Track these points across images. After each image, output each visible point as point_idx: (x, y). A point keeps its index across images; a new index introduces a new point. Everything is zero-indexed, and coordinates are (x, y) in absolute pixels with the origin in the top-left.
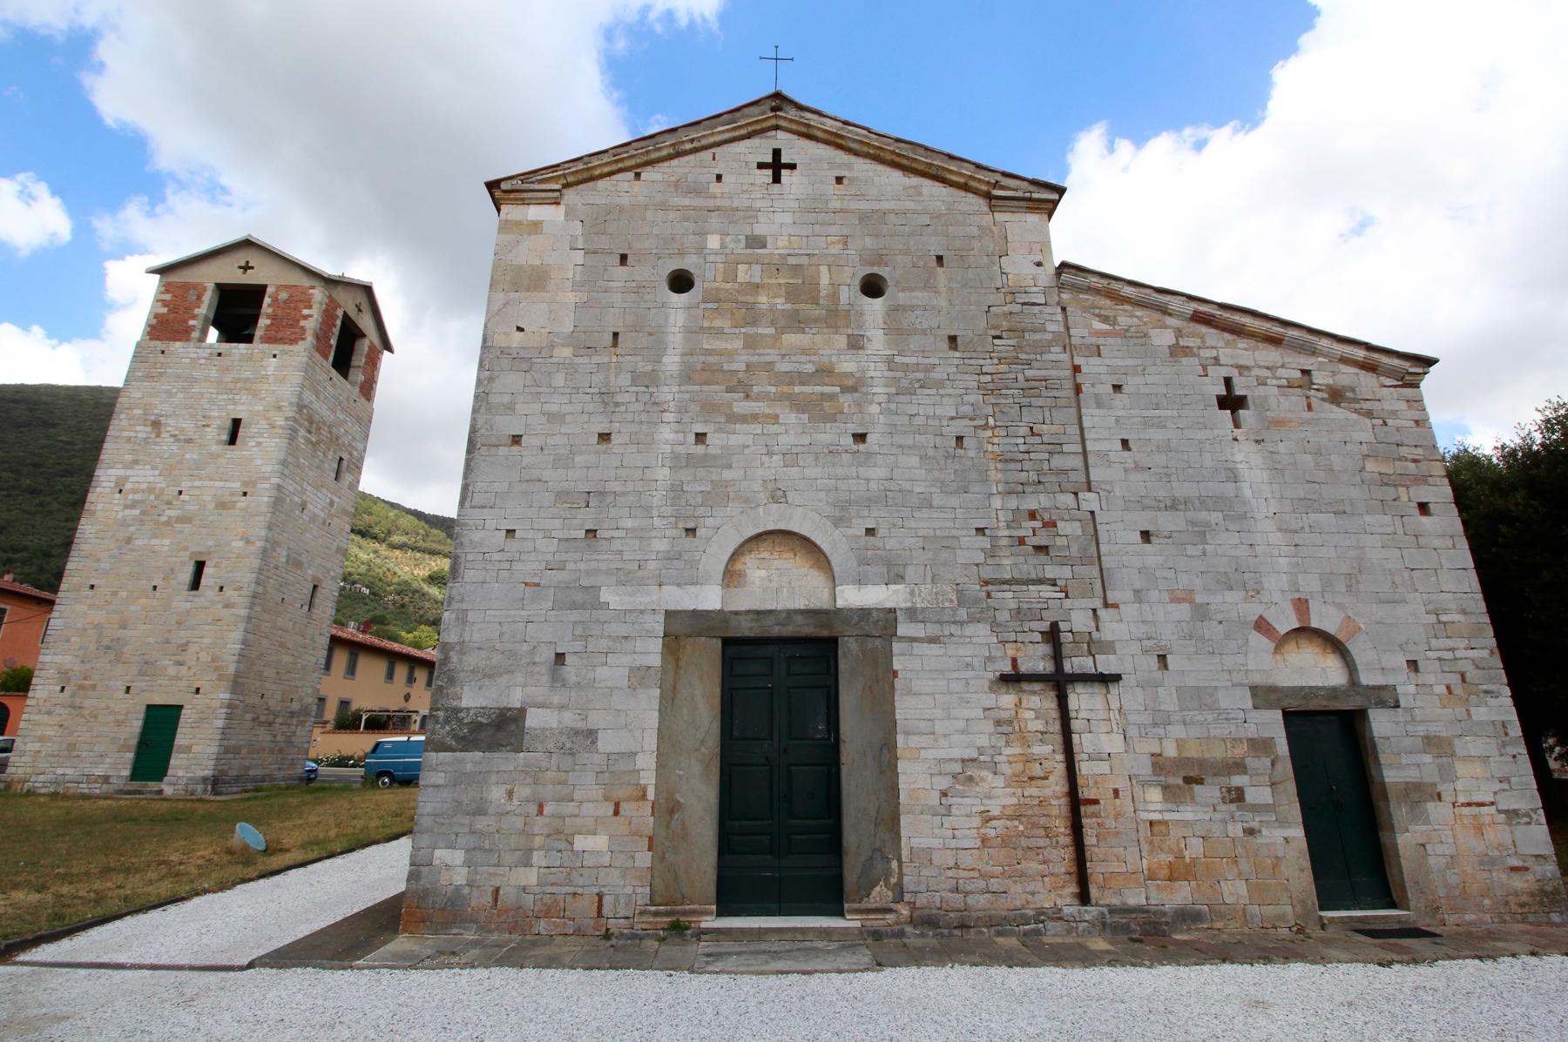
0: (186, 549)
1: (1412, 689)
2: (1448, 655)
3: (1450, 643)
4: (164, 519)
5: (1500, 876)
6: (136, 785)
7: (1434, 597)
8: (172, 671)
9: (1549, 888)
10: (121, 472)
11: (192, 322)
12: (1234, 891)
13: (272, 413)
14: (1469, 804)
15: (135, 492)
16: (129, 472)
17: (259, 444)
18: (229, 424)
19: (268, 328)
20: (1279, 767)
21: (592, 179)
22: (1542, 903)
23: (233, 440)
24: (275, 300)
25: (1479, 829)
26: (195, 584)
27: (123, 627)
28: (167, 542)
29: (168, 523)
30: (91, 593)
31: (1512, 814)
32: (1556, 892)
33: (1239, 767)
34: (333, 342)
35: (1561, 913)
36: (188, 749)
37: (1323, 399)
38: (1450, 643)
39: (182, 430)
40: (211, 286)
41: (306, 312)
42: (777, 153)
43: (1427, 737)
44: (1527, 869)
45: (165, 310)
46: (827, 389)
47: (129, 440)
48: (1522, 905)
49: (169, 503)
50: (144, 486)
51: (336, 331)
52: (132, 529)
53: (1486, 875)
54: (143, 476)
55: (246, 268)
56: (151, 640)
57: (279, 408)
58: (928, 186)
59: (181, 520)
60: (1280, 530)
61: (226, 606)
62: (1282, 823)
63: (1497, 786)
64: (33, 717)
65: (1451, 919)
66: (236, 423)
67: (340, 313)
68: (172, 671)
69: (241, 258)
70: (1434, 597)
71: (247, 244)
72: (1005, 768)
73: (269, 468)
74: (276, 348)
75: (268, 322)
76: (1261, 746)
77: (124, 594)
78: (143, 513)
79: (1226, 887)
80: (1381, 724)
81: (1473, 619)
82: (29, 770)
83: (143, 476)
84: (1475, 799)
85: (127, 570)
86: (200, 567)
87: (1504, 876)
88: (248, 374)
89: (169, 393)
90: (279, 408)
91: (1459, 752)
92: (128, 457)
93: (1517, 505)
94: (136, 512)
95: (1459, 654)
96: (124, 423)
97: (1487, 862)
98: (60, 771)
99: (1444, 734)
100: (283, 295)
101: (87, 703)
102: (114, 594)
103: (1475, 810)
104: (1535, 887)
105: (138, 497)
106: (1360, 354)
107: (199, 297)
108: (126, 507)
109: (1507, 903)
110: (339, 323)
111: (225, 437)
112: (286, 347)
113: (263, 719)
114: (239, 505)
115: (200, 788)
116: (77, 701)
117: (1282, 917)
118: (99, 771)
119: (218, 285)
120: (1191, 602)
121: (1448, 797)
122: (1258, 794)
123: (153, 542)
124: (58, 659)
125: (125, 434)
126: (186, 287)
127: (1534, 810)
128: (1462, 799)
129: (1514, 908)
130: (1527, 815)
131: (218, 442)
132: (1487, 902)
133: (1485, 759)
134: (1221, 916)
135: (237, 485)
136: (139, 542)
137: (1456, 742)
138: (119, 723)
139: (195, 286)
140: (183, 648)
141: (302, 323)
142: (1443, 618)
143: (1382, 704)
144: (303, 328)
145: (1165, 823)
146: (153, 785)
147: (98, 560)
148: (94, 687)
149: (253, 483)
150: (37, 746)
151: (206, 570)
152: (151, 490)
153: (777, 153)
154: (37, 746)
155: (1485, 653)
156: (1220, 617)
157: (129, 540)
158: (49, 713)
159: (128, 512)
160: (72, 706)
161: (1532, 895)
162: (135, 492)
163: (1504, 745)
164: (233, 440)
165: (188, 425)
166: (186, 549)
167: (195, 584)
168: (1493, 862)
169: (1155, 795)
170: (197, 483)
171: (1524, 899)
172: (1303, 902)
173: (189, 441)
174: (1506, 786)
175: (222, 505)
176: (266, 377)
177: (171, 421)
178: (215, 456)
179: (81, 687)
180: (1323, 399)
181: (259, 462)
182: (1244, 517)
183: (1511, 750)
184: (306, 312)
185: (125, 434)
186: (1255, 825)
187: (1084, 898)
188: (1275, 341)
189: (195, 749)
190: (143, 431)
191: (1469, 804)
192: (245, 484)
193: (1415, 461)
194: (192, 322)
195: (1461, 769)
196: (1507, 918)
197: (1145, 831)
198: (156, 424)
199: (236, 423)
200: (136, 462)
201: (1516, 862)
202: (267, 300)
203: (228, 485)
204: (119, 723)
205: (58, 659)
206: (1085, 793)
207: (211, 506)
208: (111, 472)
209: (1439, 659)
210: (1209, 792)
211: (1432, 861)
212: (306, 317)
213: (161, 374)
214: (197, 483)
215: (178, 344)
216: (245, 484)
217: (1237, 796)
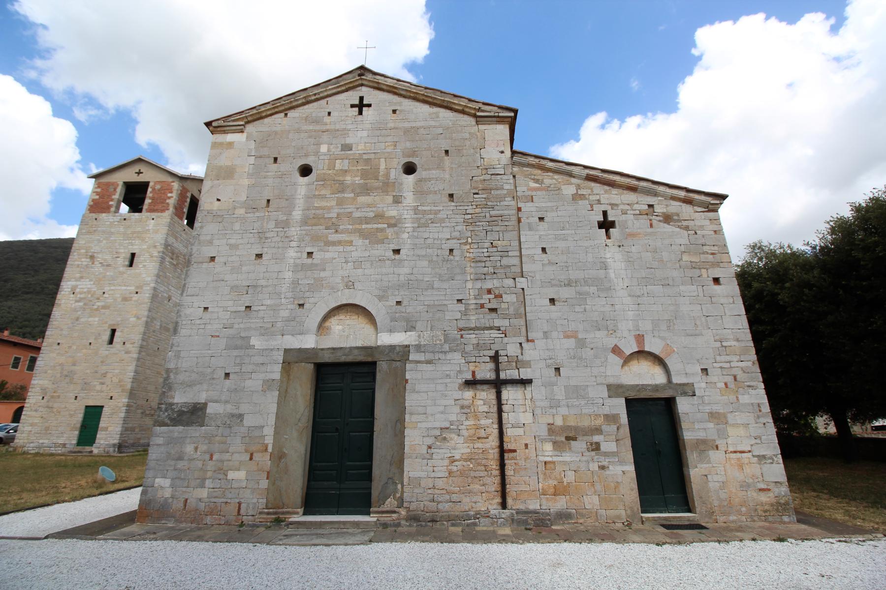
1: (703, 385)
2: (727, 365)
3: (728, 358)
4: (95, 307)
5: (752, 494)
6: (80, 448)
7: (720, 332)
8: (98, 388)
9: (782, 501)
10: (74, 283)
11: (111, 203)
12: (591, 501)
13: (151, 250)
14: (735, 452)
15: (81, 293)
16: (78, 283)
17: (144, 266)
18: (129, 256)
19: (150, 204)
20: (621, 431)
21: (262, 118)
22: (777, 510)
23: (131, 265)
24: (154, 189)
25: (741, 467)
26: (111, 342)
27: (74, 365)
28: (97, 319)
29: (97, 310)
30: (58, 347)
31: (762, 458)
32: (787, 504)
33: (598, 430)
34: (186, 210)
35: (789, 516)
36: (106, 429)
37: (660, 221)
38: (728, 358)
39: (105, 260)
40: (121, 183)
41: (169, 195)
42: (361, 98)
43: (711, 413)
44: (769, 490)
45: (97, 197)
46: (380, 226)
47: (78, 266)
48: (765, 511)
49: (98, 299)
50: (85, 290)
51: (187, 204)
52: (79, 313)
53: (744, 493)
54: (85, 285)
55: (139, 173)
56: (88, 371)
57: (155, 247)
58: (443, 113)
59: (104, 307)
60: (630, 296)
61: (126, 353)
62: (622, 462)
63: (753, 441)
65: (721, 519)
66: (133, 255)
67: (189, 195)
68: (98, 388)
69: (136, 168)
70: (720, 332)
71: (139, 160)
72: (465, 433)
73: (149, 279)
74: (154, 215)
75: (150, 201)
76: (611, 418)
77: (75, 347)
78: (85, 304)
79: (586, 499)
80: (683, 405)
81: (743, 344)
82: (26, 441)
83: (85, 285)
84: (739, 449)
85: (76, 335)
86: (113, 331)
87: (755, 494)
88: (139, 229)
89: (99, 241)
90: (155, 247)
91: (730, 421)
92: (78, 275)
93: (814, 277)
94: (81, 304)
95: (733, 364)
96: (76, 257)
97: (745, 486)
98: (41, 441)
99: (722, 411)
100: (158, 187)
101: (55, 405)
102: (70, 347)
103: (739, 455)
104: (774, 500)
105: (82, 296)
106: (682, 194)
107: (115, 190)
108: (77, 301)
109: (756, 510)
110: (188, 200)
111: (127, 263)
112: (159, 214)
113: (148, 412)
114: (134, 299)
115: (111, 449)
116: (50, 404)
117: (619, 517)
118: (61, 441)
119: (124, 183)
120: (576, 337)
121: (722, 448)
122: (608, 446)
123: (91, 319)
124: (41, 382)
125: (77, 263)
126: (108, 184)
127: (776, 456)
128: (731, 449)
129: (761, 513)
130: (771, 458)
131: (124, 266)
132: (744, 509)
133: (746, 426)
134: (583, 516)
135: (133, 288)
136: (82, 320)
137: (729, 415)
138: (71, 416)
139: (113, 184)
140: (104, 375)
141: (168, 201)
142: (724, 344)
143: (685, 394)
144: (168, 204)
145: (554, 463)
146: (88, 449)
147: (62, 330)
148: (59, 397)
149: (141, 287)
150: (30, 428)
151: (117, 334)
152: (89, 292)
153: (361, 98)
154: (30, 428)
155: (750, 364)
156: (592, 346)
157: (77, 319)
158: (36, 411)
159: (77, 304)
160: (48, 407)
161: (772, 505)
162: (81, 293)
163: (758, 417)
164: (131, 265)
165: (108, 257)
166: (106, 323)
167: (111, 342)
168: (748, 485)
169: (548, 447)
170: (113, 288)
171: (766, 507)
172: (631, 508)
173: (108, 265)
174: (758, 441)
175: (125, 299)
176: (148, 230)
177: (100, 256)
178: (122, 273)
179: (52, 397)
180: (660, 221)
181: (144, 276)
182: (609, 289)
183: (763, 420)
184: (169, 195)
185: (77, 263)
186: (605, 463)
187: (504, 505)
188: (633, 189)
189: (110, 429)
190: (85, 261)
191: (735, 452)
192: (137, 287)
193: (713, 254)
194: (111, 203)
195: (731, 431)
196: (756, 518)
197: (541, 467)
199: (133, 255)
200: (82, 278)
201: (763, 486)
202: (150, 190)
203: (129, 288)
204: (71, 416)
205: (41, 382)
206: (506, 446)
207: (119, 300)
208: (69, 283)
209: (721, 368)
210: (580, 445)
211: (711, 485)
212: (169, 198)
214: (113, 288)
215: (104, 215)
216: (137, 287)
217: (596, 447)
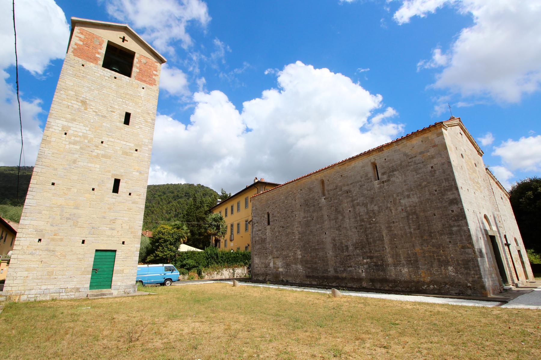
0: (109, 172)
4: (94, 154)
6: (95, 292)
8: (109, 233)
10: (65, 123)
16: (70, 125)
17: (141, 128)
24: (140, 61)
27: (77, 208)
29: (97, 156)
36: (122, 271)
45: (81, 43)
47: (68, 107)
50: (81, 134)
56: (95, 216)
59: (104, 156)
61: (133, 203)
64: (20, 256)
68: (109, 233)
69: (123, 34)
71: (125, 29)
78: (81, 148)
82: (22, 288)
83: (77, 128)
90: (149, 114)
98: (44, 287)
102: (69, 189)
105: (78, 139)
108: (70, 143)
115: (132, 290)
116: (51, 248)
118: (70, 286)
119: (109, 41)
123: (89, 165)
124: (34, 223)
126: (93, 36)
131: (120, 122)
135: (133, 145)
138: (80, 260)
139: (98, 38)
140: (114, 221)
141: (154, 77)
146: (105, 291)
148: (61, 240)
150: (25, 274)
151: (121, 184)
154: (25, 274)
157: (75, 162)
158: (32, 254)
159: (72, 146)
162: (76, 136)
166: (109, 172)
173: (104, 117)
175: (125, 153)
179: (53, 240)
188: (501, 188)
189: (125, 271)
198: (84, 103)
200: (74, 120)
203: (127, 144)
204: (80, 260)
205: (34, 223)
213: (83, 77)
214: (111, 139)
215: (92, 64)
